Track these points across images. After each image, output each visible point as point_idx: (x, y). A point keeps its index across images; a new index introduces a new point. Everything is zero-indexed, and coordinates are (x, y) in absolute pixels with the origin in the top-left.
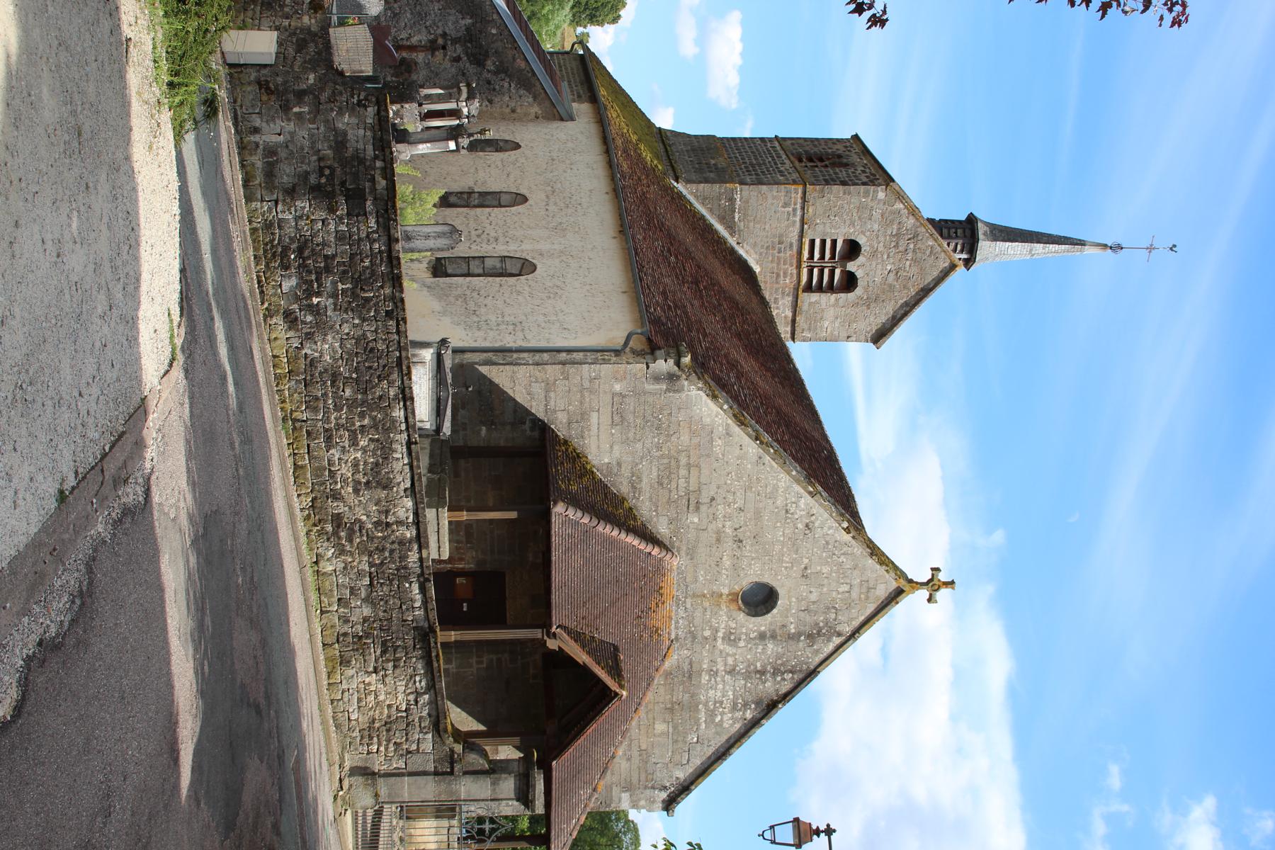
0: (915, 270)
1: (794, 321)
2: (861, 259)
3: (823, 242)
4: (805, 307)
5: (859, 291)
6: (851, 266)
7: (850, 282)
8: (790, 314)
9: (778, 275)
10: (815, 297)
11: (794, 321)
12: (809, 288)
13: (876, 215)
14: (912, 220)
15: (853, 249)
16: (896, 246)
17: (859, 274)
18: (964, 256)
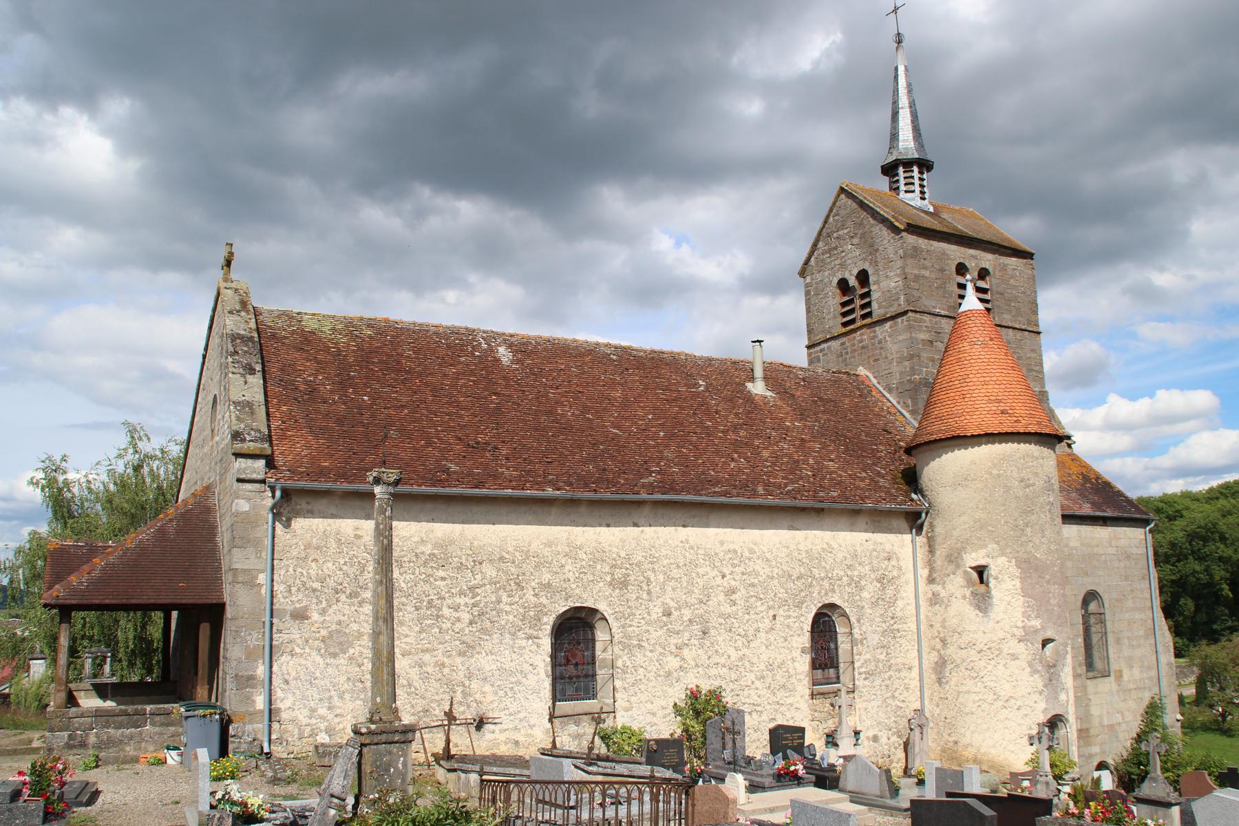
0: (849, 223)
1: (893, 318)
2: (847, 276)
3: (844, 315)
4: (882, 311)
5: (866, 266)
6: (853, 282)
7: (863, 277)
8: (889, 324)
9: (863, 347)
10: (875, 305)
11: (893, 318)
12: (869, 314)
13: (819, 277)
14: (821, 244)
15: (843, 285)
16: (836, 248)
17: (855, 272)
18: (901, 170)
